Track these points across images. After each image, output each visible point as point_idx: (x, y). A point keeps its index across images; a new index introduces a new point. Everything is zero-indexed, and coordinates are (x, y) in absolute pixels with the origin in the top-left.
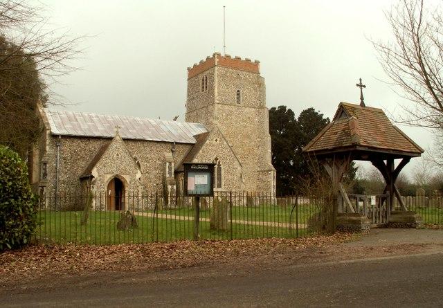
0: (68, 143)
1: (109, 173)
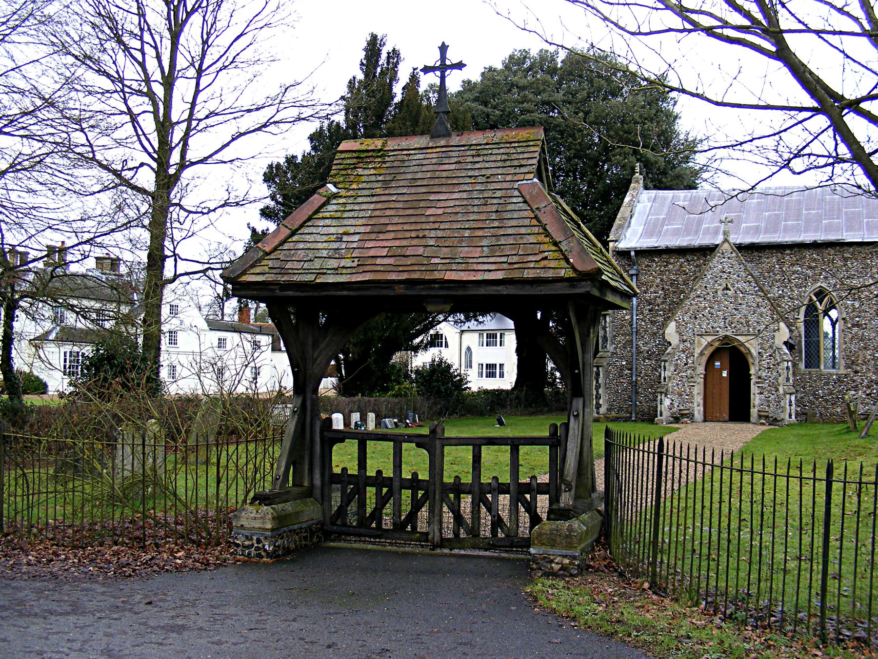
0: (656, 265)
1: (707, 333)
